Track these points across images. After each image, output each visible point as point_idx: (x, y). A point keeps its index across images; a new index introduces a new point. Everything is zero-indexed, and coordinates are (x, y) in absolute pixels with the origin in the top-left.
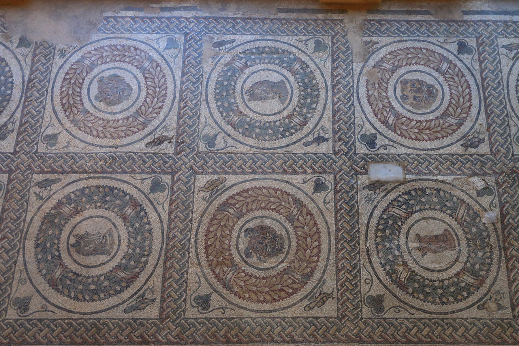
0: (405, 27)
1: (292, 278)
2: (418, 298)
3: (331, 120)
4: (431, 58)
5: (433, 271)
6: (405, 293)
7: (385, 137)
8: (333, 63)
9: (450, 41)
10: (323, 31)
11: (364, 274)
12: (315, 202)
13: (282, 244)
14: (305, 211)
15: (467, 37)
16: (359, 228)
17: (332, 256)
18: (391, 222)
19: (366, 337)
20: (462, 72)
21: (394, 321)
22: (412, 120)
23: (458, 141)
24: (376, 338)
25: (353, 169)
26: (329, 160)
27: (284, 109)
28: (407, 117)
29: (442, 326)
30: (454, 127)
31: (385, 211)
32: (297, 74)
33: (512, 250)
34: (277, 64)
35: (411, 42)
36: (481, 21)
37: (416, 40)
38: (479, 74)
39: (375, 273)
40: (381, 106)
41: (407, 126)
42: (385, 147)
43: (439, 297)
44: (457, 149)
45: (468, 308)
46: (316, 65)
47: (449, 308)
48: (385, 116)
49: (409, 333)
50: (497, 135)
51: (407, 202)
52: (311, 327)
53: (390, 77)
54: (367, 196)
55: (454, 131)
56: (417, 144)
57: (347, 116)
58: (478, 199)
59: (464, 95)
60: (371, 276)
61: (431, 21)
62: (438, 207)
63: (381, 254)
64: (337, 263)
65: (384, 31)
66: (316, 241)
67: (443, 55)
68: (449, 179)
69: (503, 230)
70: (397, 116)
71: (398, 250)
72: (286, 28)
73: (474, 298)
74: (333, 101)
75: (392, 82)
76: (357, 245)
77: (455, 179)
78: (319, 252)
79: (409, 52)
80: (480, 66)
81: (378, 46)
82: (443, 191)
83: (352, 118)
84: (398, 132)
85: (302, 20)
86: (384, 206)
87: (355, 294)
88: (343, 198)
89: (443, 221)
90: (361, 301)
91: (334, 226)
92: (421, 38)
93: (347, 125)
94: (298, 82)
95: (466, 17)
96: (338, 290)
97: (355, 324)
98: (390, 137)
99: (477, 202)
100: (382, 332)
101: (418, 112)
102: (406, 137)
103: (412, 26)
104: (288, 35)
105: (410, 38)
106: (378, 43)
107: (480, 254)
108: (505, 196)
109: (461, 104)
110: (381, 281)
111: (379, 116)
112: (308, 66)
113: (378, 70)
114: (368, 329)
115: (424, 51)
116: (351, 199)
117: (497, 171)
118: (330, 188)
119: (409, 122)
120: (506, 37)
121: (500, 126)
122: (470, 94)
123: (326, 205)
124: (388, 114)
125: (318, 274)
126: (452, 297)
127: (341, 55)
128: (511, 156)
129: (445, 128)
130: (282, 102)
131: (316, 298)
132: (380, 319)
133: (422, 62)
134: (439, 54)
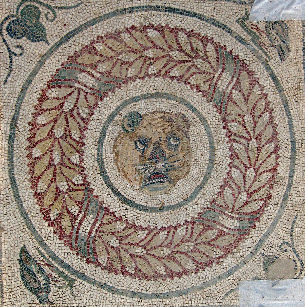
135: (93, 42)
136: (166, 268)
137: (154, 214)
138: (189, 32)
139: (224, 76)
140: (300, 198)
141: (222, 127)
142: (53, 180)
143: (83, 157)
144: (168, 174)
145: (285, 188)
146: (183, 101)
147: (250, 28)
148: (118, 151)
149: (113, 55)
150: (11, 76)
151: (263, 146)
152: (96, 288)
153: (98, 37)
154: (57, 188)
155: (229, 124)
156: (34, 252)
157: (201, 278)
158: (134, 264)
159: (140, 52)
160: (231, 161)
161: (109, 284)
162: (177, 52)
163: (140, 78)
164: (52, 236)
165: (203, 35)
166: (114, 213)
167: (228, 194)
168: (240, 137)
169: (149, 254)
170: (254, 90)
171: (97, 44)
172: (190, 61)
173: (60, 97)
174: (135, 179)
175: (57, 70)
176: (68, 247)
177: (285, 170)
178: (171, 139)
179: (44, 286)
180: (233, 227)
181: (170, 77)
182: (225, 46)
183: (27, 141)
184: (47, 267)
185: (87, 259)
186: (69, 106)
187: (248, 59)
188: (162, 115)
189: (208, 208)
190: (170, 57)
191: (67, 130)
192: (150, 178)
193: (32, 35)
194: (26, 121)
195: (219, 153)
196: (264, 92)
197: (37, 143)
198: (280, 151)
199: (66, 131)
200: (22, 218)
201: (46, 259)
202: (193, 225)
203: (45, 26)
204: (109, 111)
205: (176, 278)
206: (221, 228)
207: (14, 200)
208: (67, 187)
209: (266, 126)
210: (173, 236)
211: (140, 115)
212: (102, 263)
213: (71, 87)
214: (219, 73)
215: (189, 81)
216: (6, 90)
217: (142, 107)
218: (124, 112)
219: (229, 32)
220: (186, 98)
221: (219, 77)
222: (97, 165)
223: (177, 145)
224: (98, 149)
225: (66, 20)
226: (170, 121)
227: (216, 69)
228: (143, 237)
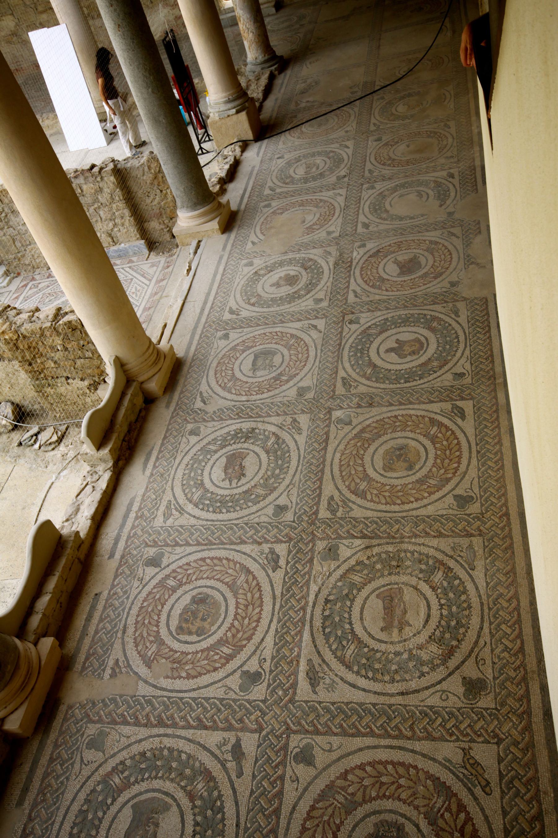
0: (107, 624)
1: (442, 811)
2: (465, 636)
3: (210, 732)
4: (157, 597)
5: (429, 616)
6: (458, 650)
7: (248, 660)
8: (128, 724)
9: (142, 575)
10: (76, 735)
11: (434, 701)
12: (329, 766)
13: (390, 824)
14: (340, 783)
15: (141, 556)
16: (370, 703)
17: (408, 744)
18: (364, 661)
19: (521, 706)
20: (184, 565)
21: (496, 666)
22: (232, 625)
23: (268, 576)
24: (521, 692)
25: (286, 706)
26: (269, 739)
27: (178, 805)
28: (227, 631)
29: (498, 610)
30: (250, 578)
31: (349, 667)
32: (129, 781)
34: (105, 813)
35: (129, 619)
36: (127, 542)
37: (128, 613)
38: (191, 547)
39: (433, 685)
40: (206, 662)
41: (238, 631)
42: (262, 661)
43: (463, 611)
44: (278, 576)
45: (473, 580)
46: (123, 749)
47: (475, 601)
48: (220, 658)
49: (511, 650)
51: (339, 639)
52: (515, 786)
53: (169, 647)
54: (327, 689)
55: (254, 578)
56: (264, 622)
57: (209, 709)
58: (341, 560)
59: (212, 564)
60: (436, 692)
61: (109, 594)
62: (348, 603)
63: (407, 677)
64: (419, 739)
65: (104, 651)
66: (386, 768)
67: (157, 584)
68: (314, 588)
69: (380, 538)
70: (222, 643)
71: (402, 654)
72: (52, 795)
73: (462, 574)
74: (183, 728)
75: (176, 646)
76: (393, 708)
77: (315, 582)
78: (402, 764)
79: (141, 622)
80: (181, 546)
81: (122, 659)
82: (328, 596)
83: (214, 702)
84: (244, 642)
85: (47, 769)
86: (342, 667)
87: (462, 716)
88: (326, 723)
89: (367, 598)
90: (472, 709)
91: (365, 738)
92: (128, 606)
93: (223, 709)
94: (143, 780)
95: (117, 556)
96: (458, 740)
97: (506, 720)
98: (249, 653)
99: (345, 561)
100: (512, 683)
101: (223, 616)
102: (253, 634)
103: (109, 616)
104: (63, 793)
105: (124, 619)
106: (118, 659)
107: (408, 563)
109: (223, 569)
110: (444, 679)
111: (217, 665)
112: (122, 763)
113: (155, 662)
114: (510, 701)
115: (145, 604)
116: (328, 711)
117: (310, 538)
118: (309, 741)
119: (233, 629)
120: (154, 518)
122: (212, 559)
123: (333, 749)
124: (218, 654)
125: (434, 769)
126: (460, 596)
127: (119, 711)
129: (250, 588)
130: (166, 808)
131: (472, 774)
132: (495, 684)
133: (159, 608)
134: (154, 587)
142: (449, 445)
146: (386, 477)
217: (405, 473)
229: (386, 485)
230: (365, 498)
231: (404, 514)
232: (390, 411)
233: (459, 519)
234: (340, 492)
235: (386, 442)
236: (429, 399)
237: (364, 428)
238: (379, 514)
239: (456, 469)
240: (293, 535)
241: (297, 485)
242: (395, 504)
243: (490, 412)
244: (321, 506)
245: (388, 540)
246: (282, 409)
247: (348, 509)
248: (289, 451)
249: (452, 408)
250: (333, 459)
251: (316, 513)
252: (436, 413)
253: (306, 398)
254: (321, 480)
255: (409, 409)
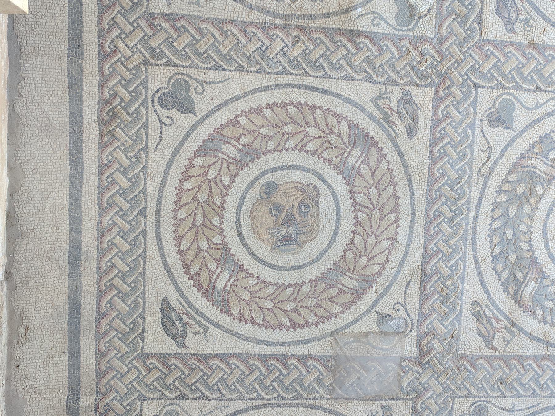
33: (283, 41)
50: (520, 62)
69: (324, 30)
108: (393, 49)
117: (446, 45)
121: (538, 71)
128: (475, 80)
135: (237, 116)
136: (291, 320)
137: (282, 272)
138: (326, 110)
139: (354, 152)
140: (416, 264)
141: (348, 197)
142: (196, 239)
143: (224, 220)
144: (297, 237)
145: (402, 255)
147: (382, 107)
148: (255, 216)
149: (255, 128)
150: (161, 144)
151: (385, 216)
152: (228, 335)
153: (242, 111)
154: (198, 246)
155: (356, 195)
156: (174, 302)
157: (321, 329)
158: (262, 315)
159: (279, 127)
160: (354, 228)
161: (239, 332)
162: (314, 128)
163: (278, 151)
164: (192, 289)
165: (338, 113)
166: (247, 270)
167: (350, 257)
168: (365, 207)
169: (276, 307)
170: (381, 165)
171: (241, 118)
172: (324, 137)
173: (205, 165)
174: (268, 240)
175: (204, 141)
176: (205, 299)
177: (403, 239)
178: (303, 207)
179: (182, 332)
180: (352, 287)
181: (305, 151)
182: (358, 124)
183: (174, 204)
184: (185, 316)
185: (221, 310)
186: (213, 174)
187: (378, 136)
188: (296, 185)
189: (331, 269)
190: (307, 133)
191: (210, 195)
192: (281, 241)
193: (181, 107)
194: (174, 186)
195: (345, 221)
196: (391, 167)
197: (182, 206)
198: (401, 221)
199: (209, 196)
200: (166, 272)
201: (185, 308)
202: (316, 284)
203: (194, 99)
204: (248, 179)
205: (298, 329)
206: (341, 287)
207: (159, 255)
208: (207, 246)
209: (389, 198)
210: (298, 292)
211: (276, 184)
212: (234, 313)
213: (215, 157)
214: (350, 148)
215: (323, 155)
216: (156, 156)
217: (279, 177)
218: (262, 181)
219: (362, 111)
220: (318, 171)
221: (350, 152)
222: (235, 227)
223: (307, 213)
224: (237, 213)
225: (214, 94)
226: (303, 191)
227: (348, 145)
228: (272, 292)
229: (314, 153)
230: (351, 125)
231: (283, 79)
232: (304, 342)
233: (188, 57)
234: (396, 145)
235: (313, 262)
236: (228, 365)
237: (354, 302)
238: (325, 84)
239: (186, 177)
240: (476, 57)
241: (475, 173)
242: (298, 106)
243: (114, 314)
244: (429, 116)
245: (312, 24)
246: (515, 375)
247: (381, 102)
248: (495, 258)
249: (184, 335)
250: (412, 227)
251: (437, 100)
252: (217, 325)
253: (472, 400)
254: (433, 180)
255: (269, 344)
